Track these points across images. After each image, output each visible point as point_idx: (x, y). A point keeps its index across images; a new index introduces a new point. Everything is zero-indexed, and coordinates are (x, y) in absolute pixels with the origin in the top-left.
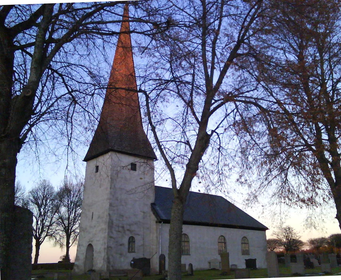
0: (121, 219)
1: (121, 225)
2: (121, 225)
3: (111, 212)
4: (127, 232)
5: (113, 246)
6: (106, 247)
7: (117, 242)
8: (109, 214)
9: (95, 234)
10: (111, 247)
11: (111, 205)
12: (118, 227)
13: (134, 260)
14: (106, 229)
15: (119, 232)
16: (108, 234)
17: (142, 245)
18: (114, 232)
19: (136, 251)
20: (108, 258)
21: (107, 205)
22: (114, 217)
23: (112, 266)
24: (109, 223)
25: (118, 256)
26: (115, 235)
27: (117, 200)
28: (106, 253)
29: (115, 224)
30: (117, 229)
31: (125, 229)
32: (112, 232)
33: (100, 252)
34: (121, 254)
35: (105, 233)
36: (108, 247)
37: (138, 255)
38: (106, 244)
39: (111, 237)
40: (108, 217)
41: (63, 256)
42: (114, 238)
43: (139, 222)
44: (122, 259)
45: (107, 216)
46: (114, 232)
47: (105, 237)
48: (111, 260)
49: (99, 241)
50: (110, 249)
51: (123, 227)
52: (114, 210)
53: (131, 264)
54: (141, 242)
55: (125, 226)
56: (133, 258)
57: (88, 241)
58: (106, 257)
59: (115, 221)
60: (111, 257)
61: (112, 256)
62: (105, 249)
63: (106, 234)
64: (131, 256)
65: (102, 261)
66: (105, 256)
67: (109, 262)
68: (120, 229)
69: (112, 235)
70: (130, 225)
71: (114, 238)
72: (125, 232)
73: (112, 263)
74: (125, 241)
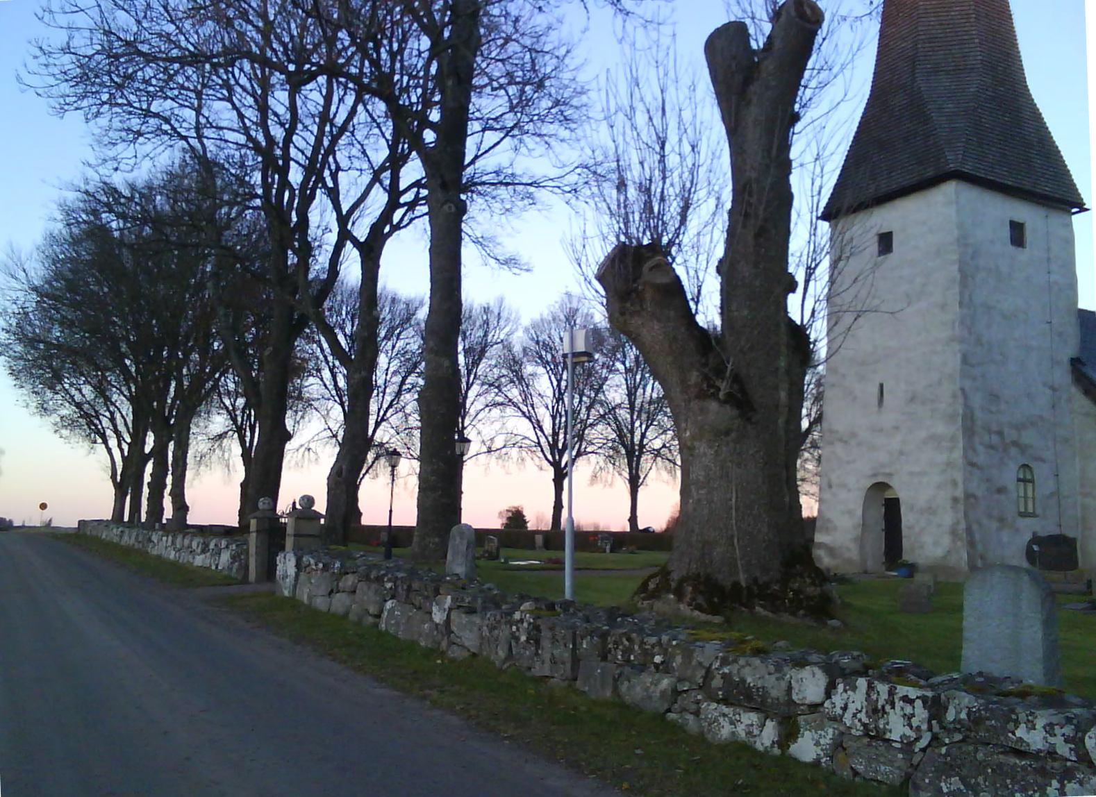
0: (994, 408)
1: (994, 427)
2: (994, 427)
3: (968, 384)
4: (1014, 451)
5: (979, 493)
6: (959, 493)
7: (988, 480)
8: (962, 389)
9: (901, 453)
10: (974, 496)
11: (965, 360)
12: (990, 432)
13: (1036, 539)
14: (953, 439)
15: (991, 447)
16: (965, 456)
17: (1052, 494)
18: (980, 449)
19: (1039, 511)
20: (969, 530)
21: (955, 362)
22: (977, 401)
23: (982, 557)
24: (964, 417)
25: (995, 525)
26: (982, 457)
27: (981, 345)
28: (961, 514)
29: (979, 423)
30: (986, 438)
31: (1008, 441)
32: (975, 450)
33: (930, 510)
34: (1001, 520)
35: (951, 450)
36: (969, 496)
37: (1047, 527)
38: (961, 486)
39: (972, 464)
40: (961, 400)
41: (508, 511)
42: (980, 468)
43: (1041, 418)
44: (1005, 536)
45: (954, 396)
46: (980, 449)
47: (949, 464)
48: (977, 537)
49: (922, 474)
50: (972, 500)
51: (1000, 433)
52: (974, 379)
53: (1030, 555)
54: (1050, 485)
55: (1006, 431)
56: (1034, 534)
57: (870, 473)
58: (963, 526)
59: (978, 414)
60: (975, 527)
61: (980, 525)
62: (955, 500)
63: (958, 454)
64: (1028, 529)
65: (946, 541)
66: (958, 523)
67: (971, 543)
68: (995, 439)
69: (975, 460)
70: (1019, 427)
71: (980, 468)
72: (1005, 450)
73: (980, 547)
74: (1009, 475)
